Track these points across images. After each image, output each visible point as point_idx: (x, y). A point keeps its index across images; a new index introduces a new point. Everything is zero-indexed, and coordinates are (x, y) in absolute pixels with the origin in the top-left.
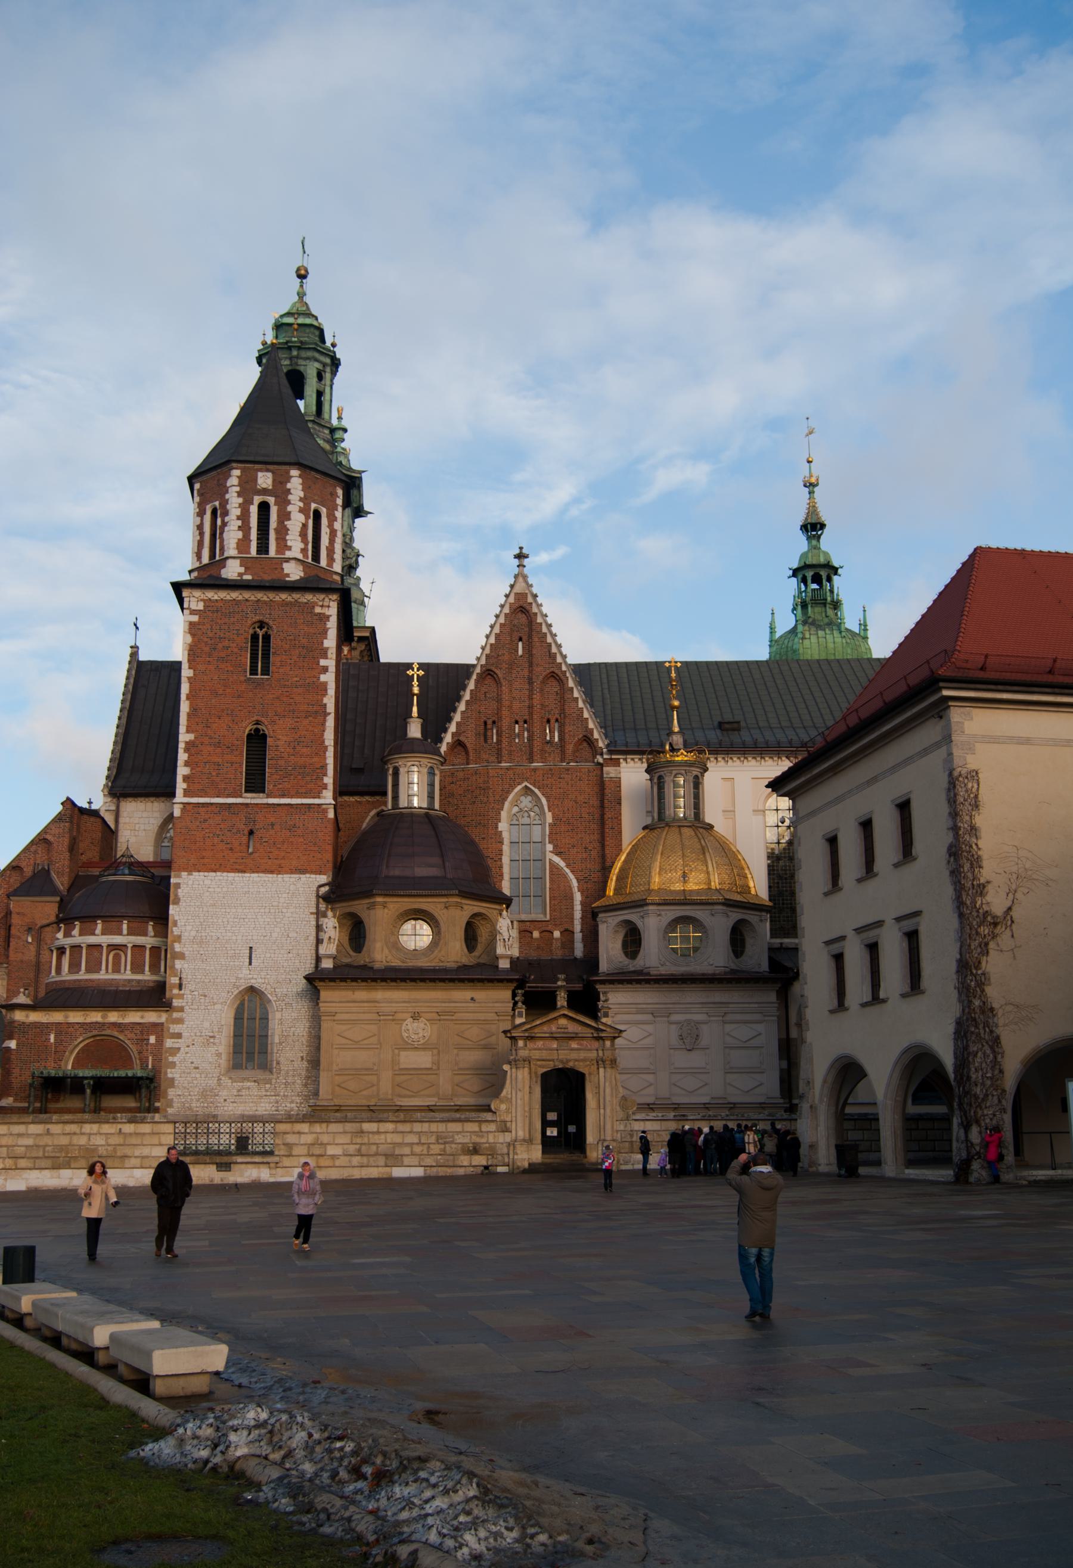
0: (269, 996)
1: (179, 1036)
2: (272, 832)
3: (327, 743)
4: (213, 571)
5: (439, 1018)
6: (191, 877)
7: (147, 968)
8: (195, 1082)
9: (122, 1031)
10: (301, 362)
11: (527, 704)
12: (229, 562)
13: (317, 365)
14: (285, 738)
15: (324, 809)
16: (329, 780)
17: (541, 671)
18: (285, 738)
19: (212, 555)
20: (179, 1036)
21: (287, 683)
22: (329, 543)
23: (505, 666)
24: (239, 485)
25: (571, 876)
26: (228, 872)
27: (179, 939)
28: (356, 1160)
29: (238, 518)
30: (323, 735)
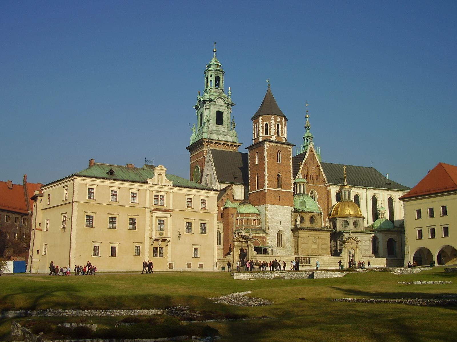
4: (268, 138)
7: (259, 225)
9: (259, 238)
10: (219, 74)
11: (312, 172)
12: (272, 136)
14: (284, 177)
16: (292, 187)
17: (315, 165)
18: (284, 177)
19: (267, 134)
20: (269, 240)
23: (309, 163)
25: (321, 209)
27: (268, 219)
28: (323, 265)
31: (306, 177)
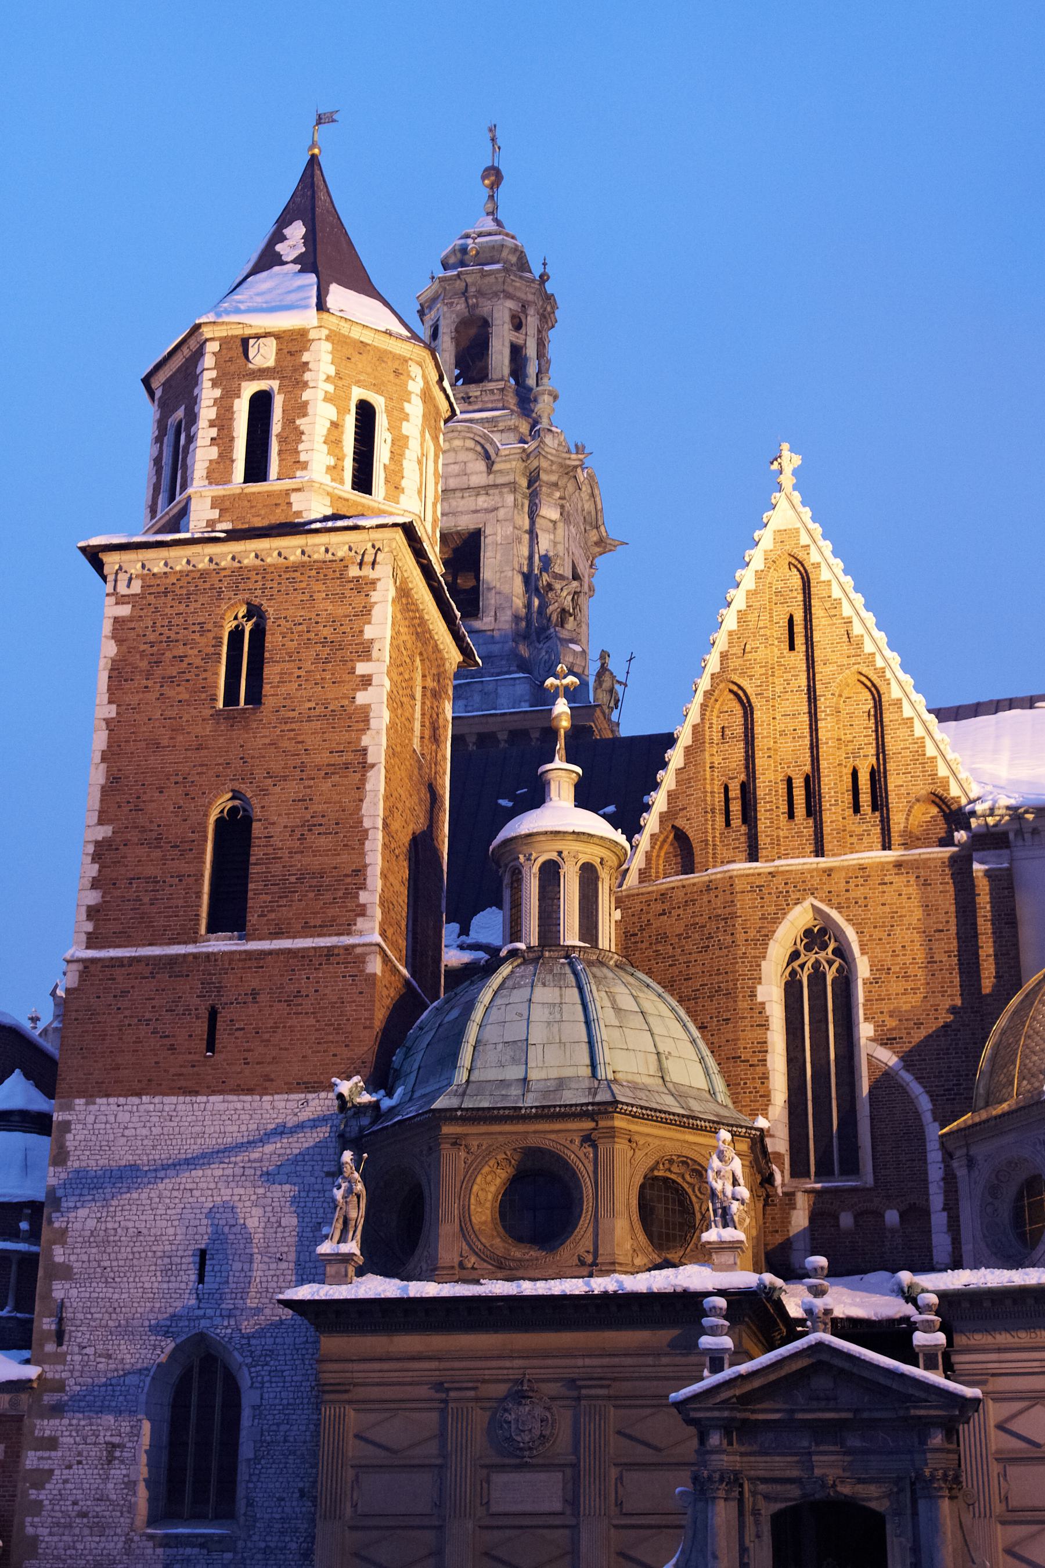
0: (236, 1353)
1: (51, 1443)
2: (253, 1009)
3: (367, 824)
5: (575, 1394)
6: (92, 1108)
8: (80, 1546)
13: (510, 304)
14: (284, 821)
15: (358, 956)
20: (51, 1443)
21: (291, 714)
22: (391, 458)
24: (217, 367)
26: (164, 1094)
29: (212, 426)
30: (360, 809)
31: (736, 807)
